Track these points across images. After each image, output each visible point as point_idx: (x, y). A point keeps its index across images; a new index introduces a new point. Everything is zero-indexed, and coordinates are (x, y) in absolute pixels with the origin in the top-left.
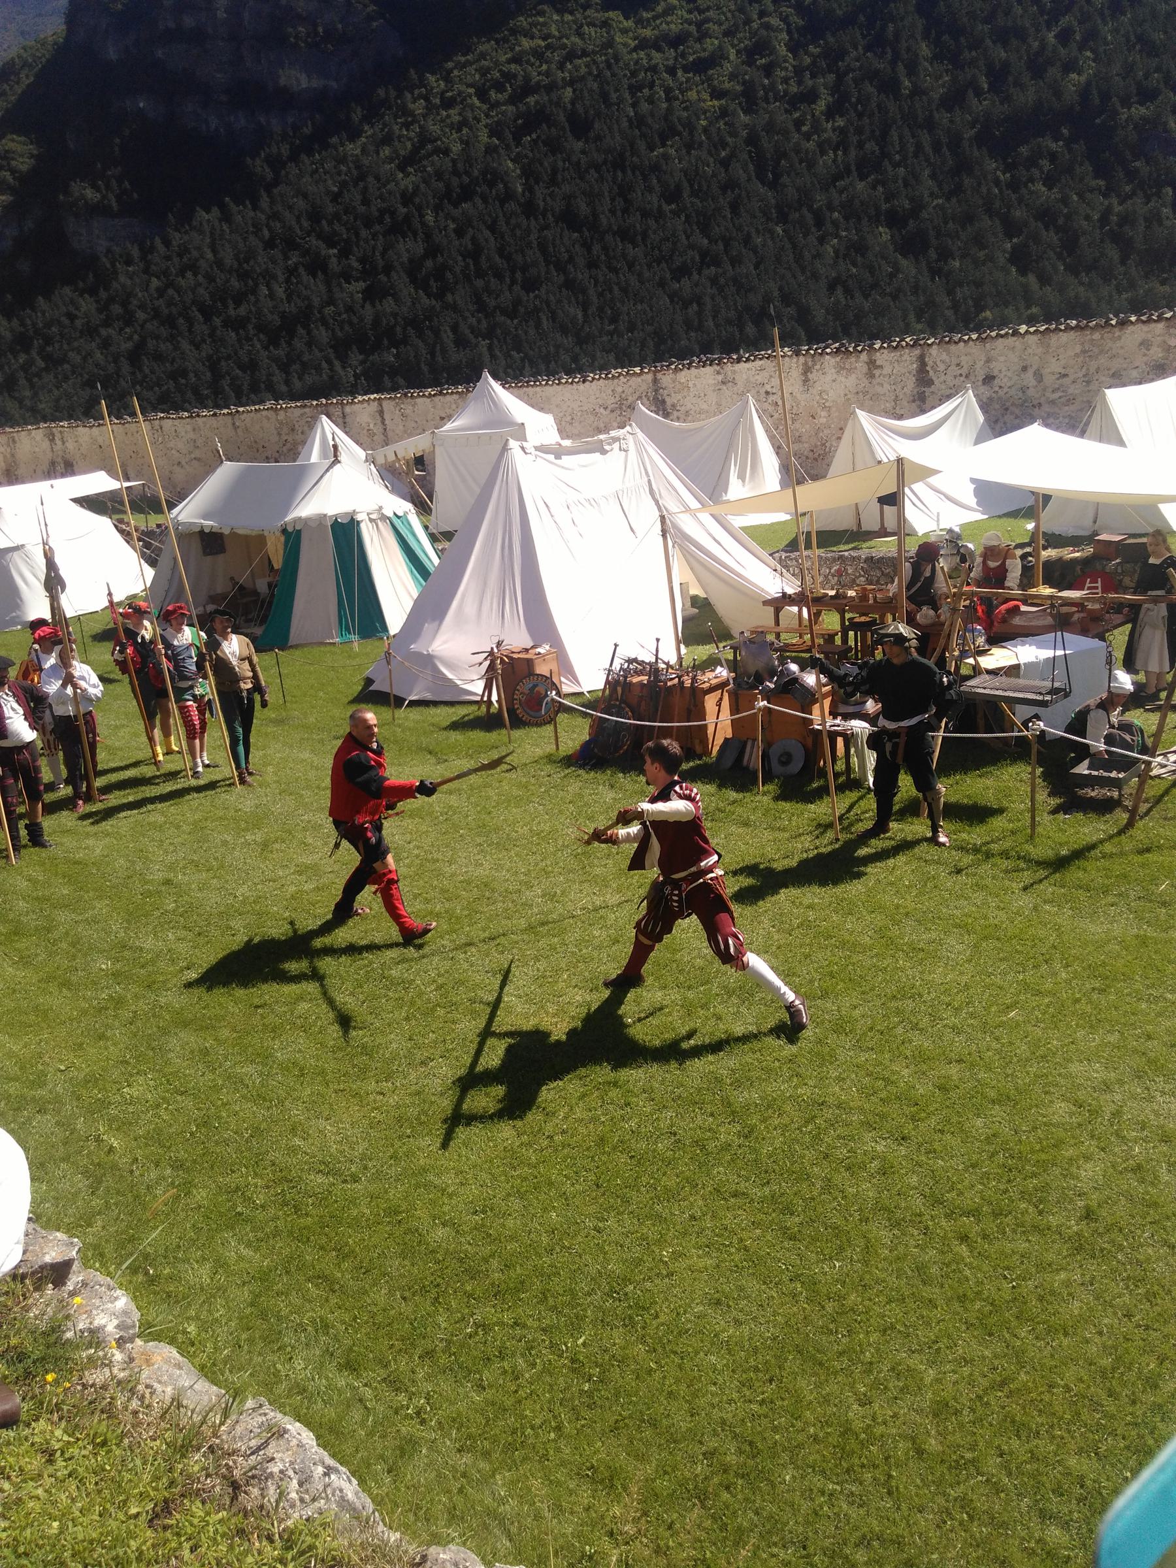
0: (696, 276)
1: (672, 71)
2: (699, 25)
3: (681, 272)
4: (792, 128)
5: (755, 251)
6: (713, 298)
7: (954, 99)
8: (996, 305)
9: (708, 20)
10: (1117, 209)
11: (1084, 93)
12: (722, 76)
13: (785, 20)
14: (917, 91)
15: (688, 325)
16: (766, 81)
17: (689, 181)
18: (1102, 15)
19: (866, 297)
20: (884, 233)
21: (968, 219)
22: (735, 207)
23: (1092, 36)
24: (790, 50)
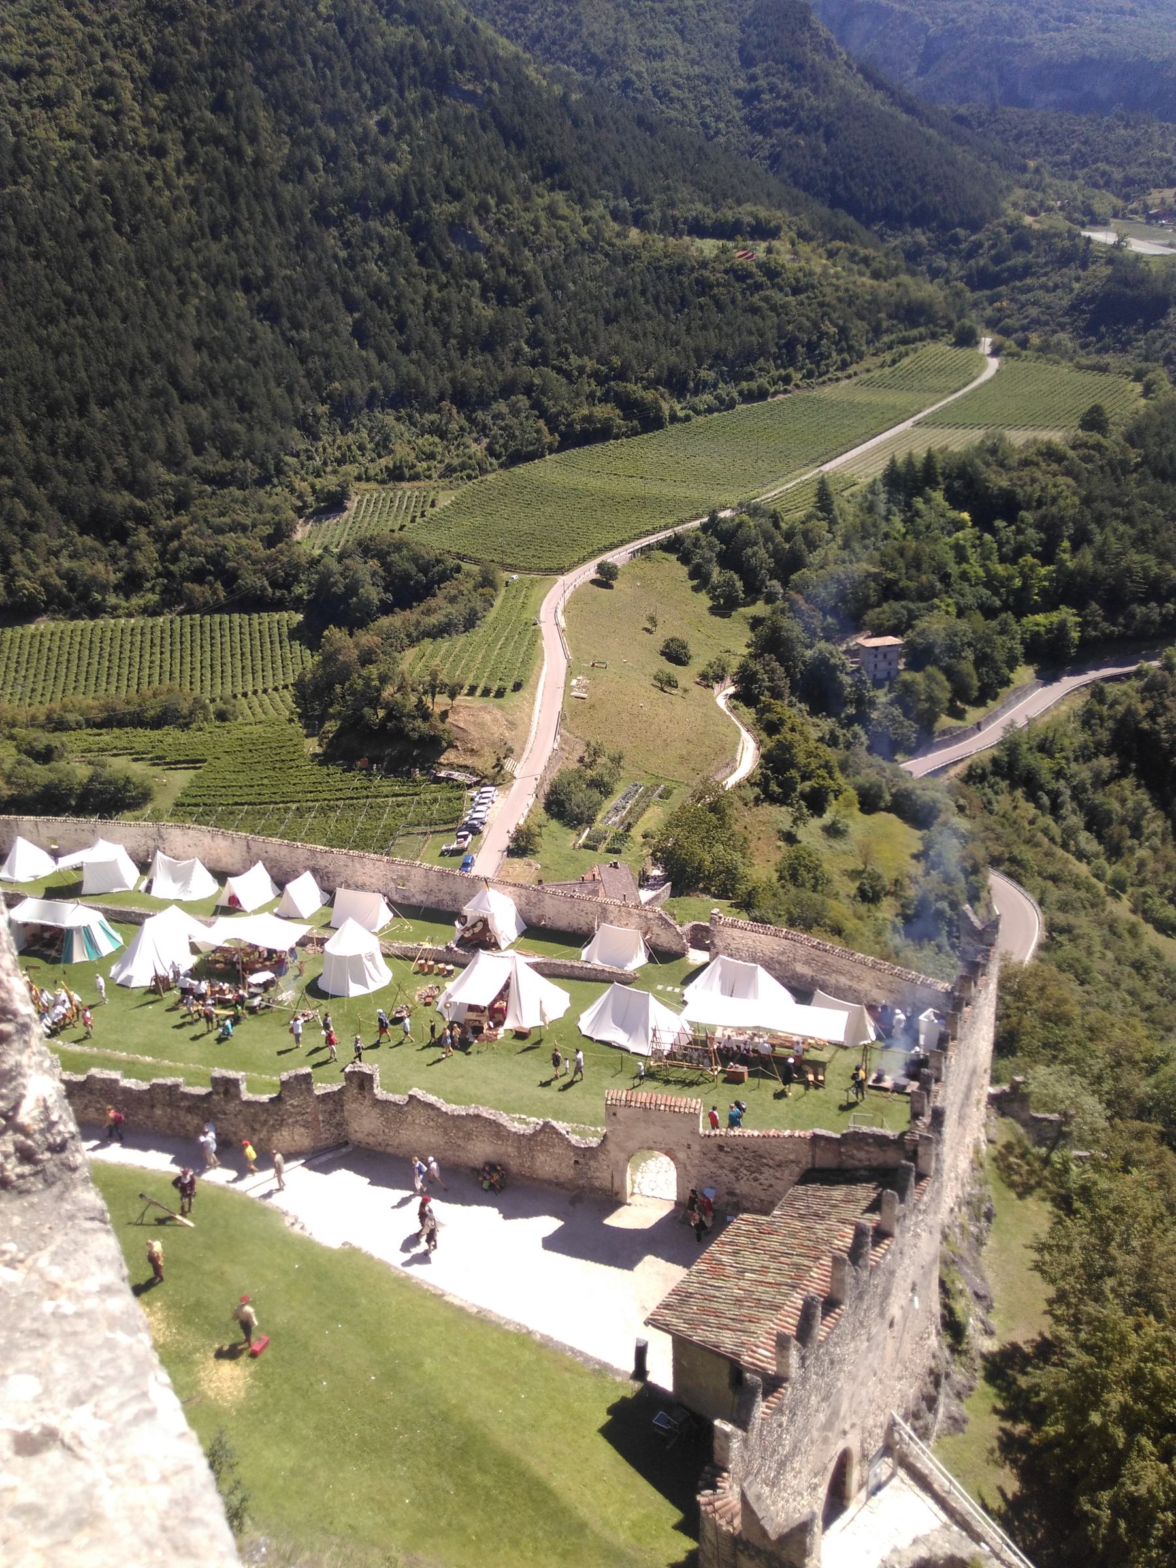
0: (63, 325)
1: (17, 105)
2: (41, 59)
3: (50, 318)
4: (144, 181)
5: (118, 303)
6: (82, 348)
7: (296, 170)
8: (343, 377)
9: (49, 56)
10: (437, 295)
11: (403, 181)
12: (69, 116)
13: (127, 66)
14: (258, 163)
15: (60, 372)
16: (115, 129)
17: (45, 225)
18: (414, 111)
19: (230, 360)
20: (240, 299)
21: (314, 291)
22: (95, 256)
23: (406, 128)
24: (134, 99)
